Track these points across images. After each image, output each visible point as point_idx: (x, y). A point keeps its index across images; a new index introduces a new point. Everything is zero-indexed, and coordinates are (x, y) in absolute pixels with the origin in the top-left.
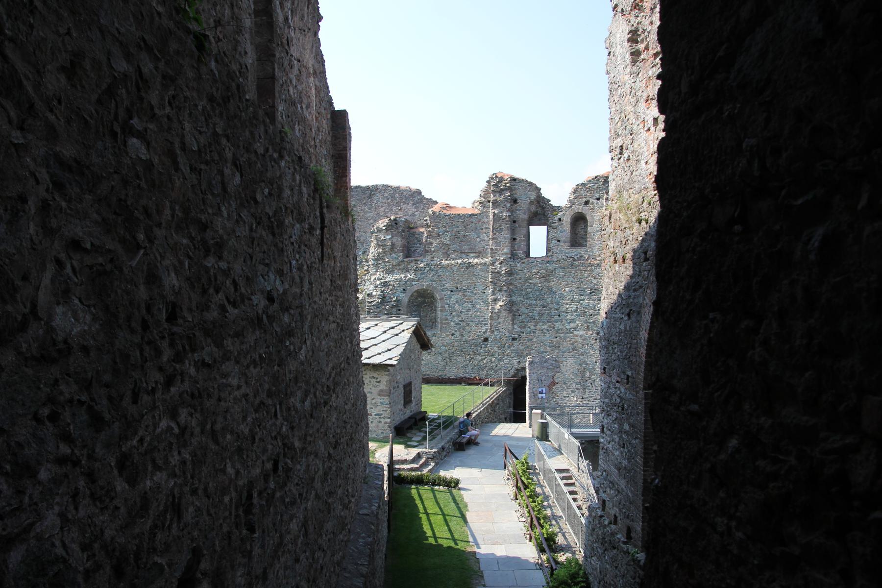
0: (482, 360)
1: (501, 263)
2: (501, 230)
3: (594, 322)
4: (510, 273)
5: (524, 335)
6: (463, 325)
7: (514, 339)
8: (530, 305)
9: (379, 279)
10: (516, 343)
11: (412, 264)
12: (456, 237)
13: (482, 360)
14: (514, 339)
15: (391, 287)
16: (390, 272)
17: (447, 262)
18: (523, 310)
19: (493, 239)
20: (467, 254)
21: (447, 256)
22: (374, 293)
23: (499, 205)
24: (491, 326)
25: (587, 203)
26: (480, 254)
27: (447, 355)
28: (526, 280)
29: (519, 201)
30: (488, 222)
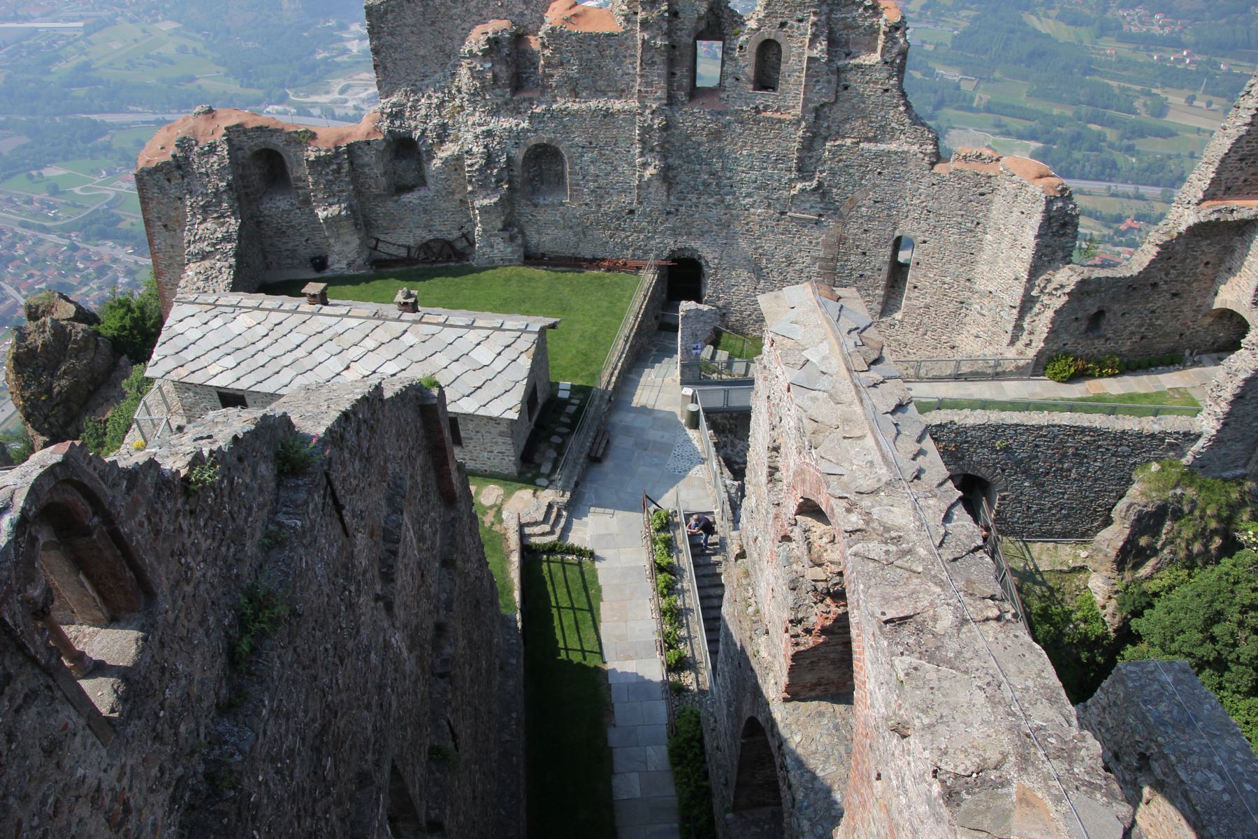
0: (627, 237)
1: (653, 113)
2: (654, 63)
3: (778, 199)
4: (666, 128)
5: (683, 209)
6: (600, 194)
7: (669, 213)
8: (693, 171)
9: (480, 125)
10: (672, 219)
11: (526, 104)
12: (586, 67)
13: (627, 237)
14: (669, 213)
15: (497, 139)
16: (495, 112)
17: (576, 107)
18: (682, 176)
19: (642, 76)
20: (604, 93)
21: (575, 93)
22: (475, 149)
23: (651, 26)
24: (639, 196)
25: (783, 25)
26: (621, 94)
27: (580, 229)
28: (688, 137)
29: (681, 15)
30: (635, 46)
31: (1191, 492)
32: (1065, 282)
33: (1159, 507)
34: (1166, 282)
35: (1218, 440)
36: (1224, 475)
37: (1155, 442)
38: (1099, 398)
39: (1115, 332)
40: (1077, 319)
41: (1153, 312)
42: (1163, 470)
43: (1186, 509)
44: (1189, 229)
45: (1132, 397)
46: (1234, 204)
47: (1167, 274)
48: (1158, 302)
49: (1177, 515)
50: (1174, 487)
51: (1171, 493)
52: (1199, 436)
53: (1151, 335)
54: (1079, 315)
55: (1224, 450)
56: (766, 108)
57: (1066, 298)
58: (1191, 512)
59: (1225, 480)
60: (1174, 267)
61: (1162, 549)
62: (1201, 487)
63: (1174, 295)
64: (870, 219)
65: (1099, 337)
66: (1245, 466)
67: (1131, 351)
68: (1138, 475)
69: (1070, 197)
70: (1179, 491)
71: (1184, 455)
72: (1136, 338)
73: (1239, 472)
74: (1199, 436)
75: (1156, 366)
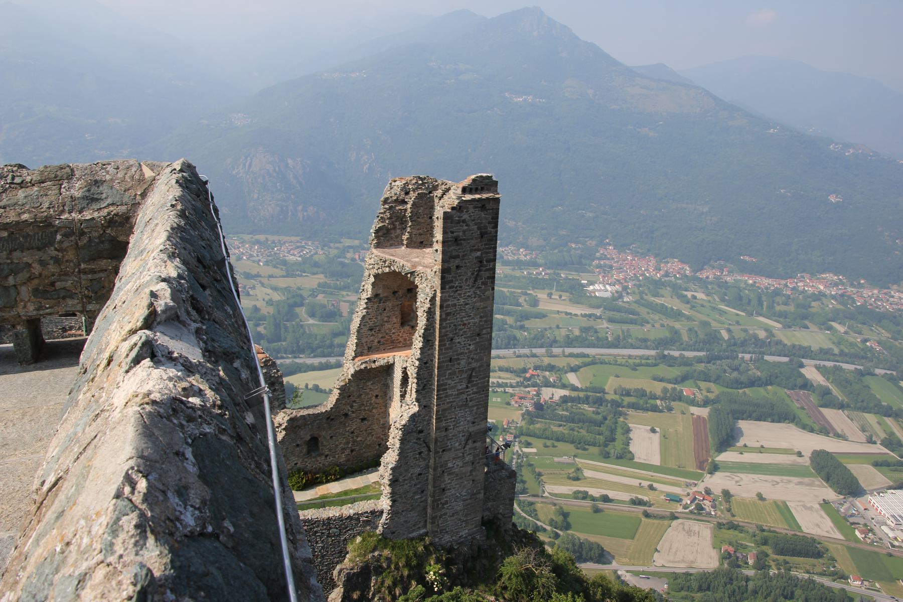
31: (386, 552)
32: (281, 421)
33: (362, 568)
34: (353, 412)
35: (394, 512)
36: (411, 536)
37: (354, 522)
38: (323, 497)
39: (330, 450)
40: (298, 445)
41: (352, 433)
42: (364, 540)
43: (385, 565)
44: (352, 375)
45: (346, 493)
46: (375, 357)
47: (352, 407)
48: (354, 425)
49: (379, 570)
50: (374, 550)
51: (370, 556)
52: (382, 512)
53: (357, 448)
55: (402, 519)
56: (71, 328)
57: (284, 433)
58: (389, 567)
59: (412, 539)
61: (373, 598)
62: (393, 548)
63: (363, 420)
65: (320, 455)
66: (425, 526)
67: (348, 460)
68: (350, 547)
69: (274, 364)
70: (376, 554)
71: (377, 527)
72: (348, 452)
73: (422, 531)
74: (382, 512)
75: (367, 468)
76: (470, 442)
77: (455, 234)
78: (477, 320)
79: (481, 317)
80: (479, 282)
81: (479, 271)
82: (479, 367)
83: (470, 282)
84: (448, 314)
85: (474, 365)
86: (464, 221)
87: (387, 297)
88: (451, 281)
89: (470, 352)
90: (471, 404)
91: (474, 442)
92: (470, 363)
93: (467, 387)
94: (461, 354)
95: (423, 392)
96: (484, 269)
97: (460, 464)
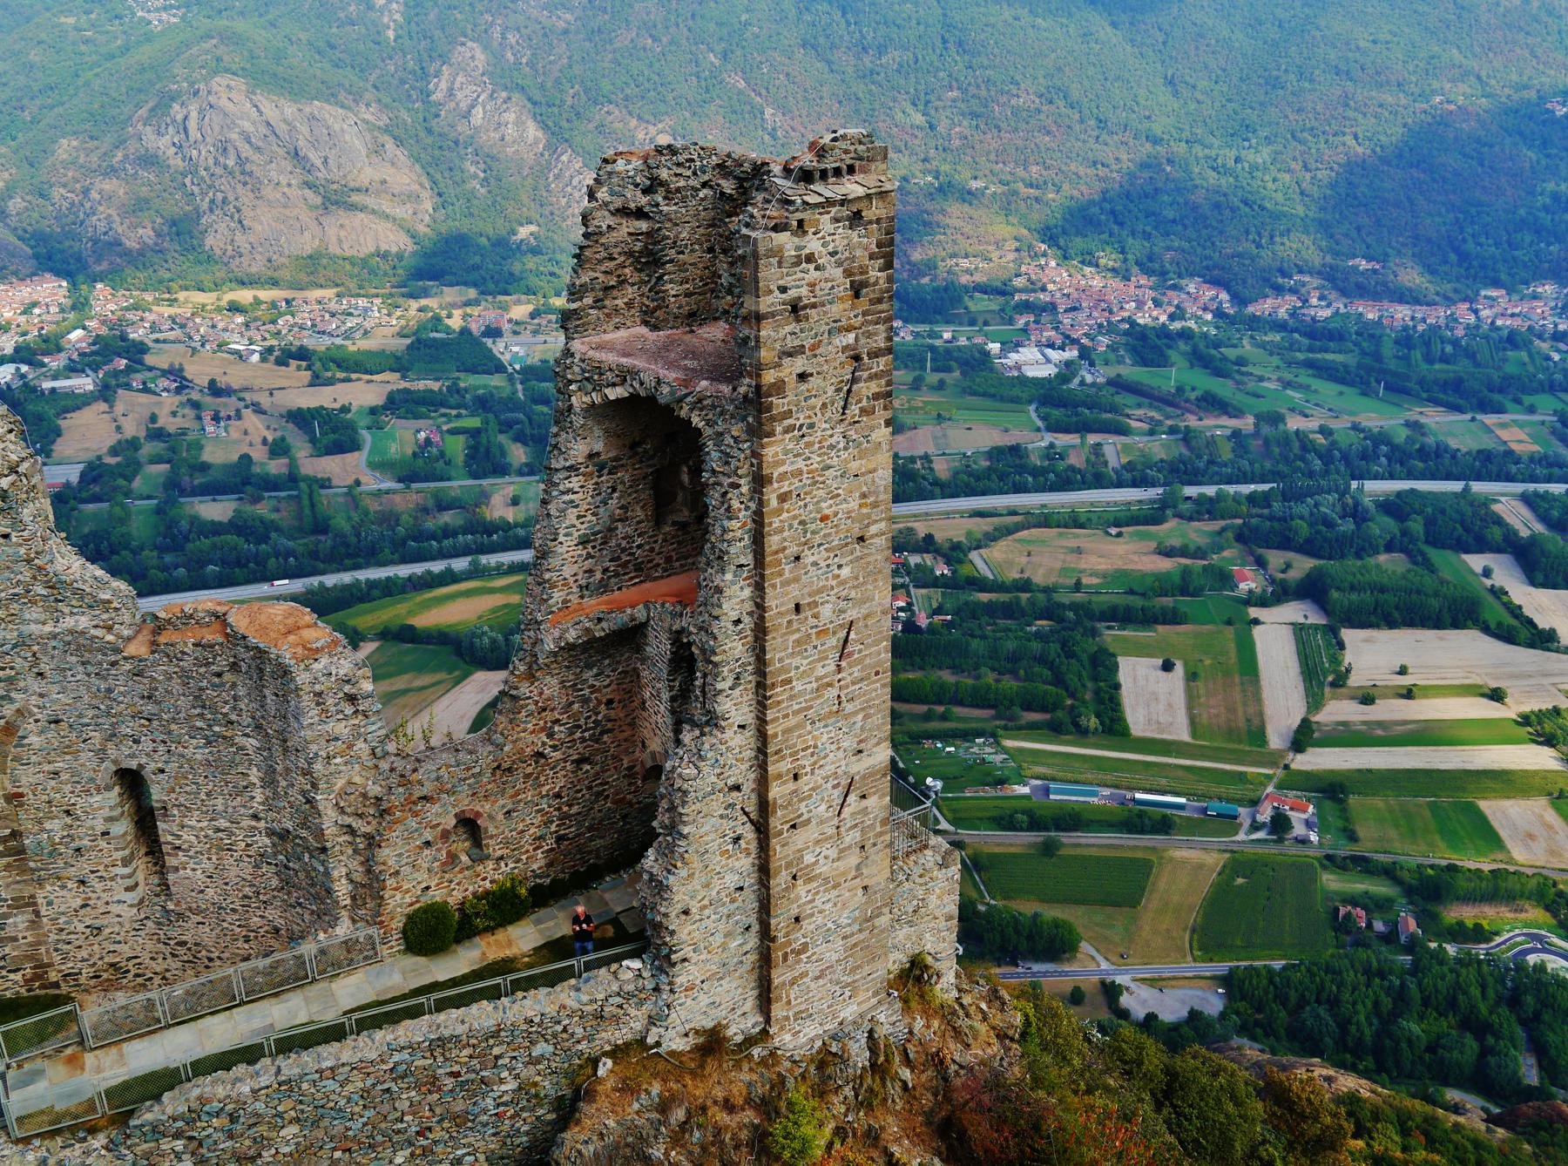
39: (506, 843)
47: (551, 735)
54: (428, 836)
60: (557, 721)
64: (47, 754)
76: (852, 798)
77: (792, 293)
78: (853, 505)
79: (864, 496)
80: (854, 410)
81: (854, 380)
82: (866, 617)
83: (833, 413)
84: (783, 498)
85: (852, 614)
86: (810, 258)
87: (615, 459)
88: (788, 414)
89: (843, 583)
90: (849, 707)
91: (864, 797)
92: (842, 611)
93: (839, 669)
94: (820, 591)
95: (737, 692)
96: (865, 374)
97: (833, 853)
